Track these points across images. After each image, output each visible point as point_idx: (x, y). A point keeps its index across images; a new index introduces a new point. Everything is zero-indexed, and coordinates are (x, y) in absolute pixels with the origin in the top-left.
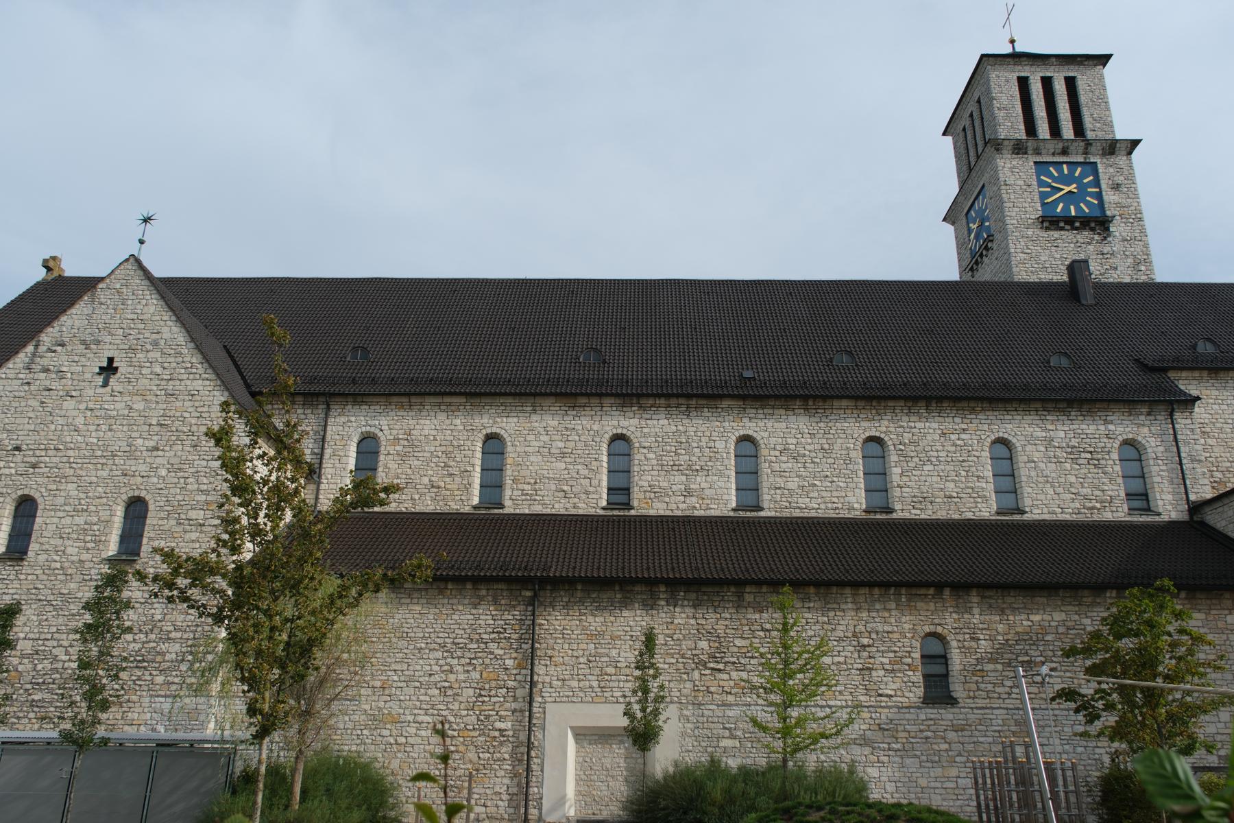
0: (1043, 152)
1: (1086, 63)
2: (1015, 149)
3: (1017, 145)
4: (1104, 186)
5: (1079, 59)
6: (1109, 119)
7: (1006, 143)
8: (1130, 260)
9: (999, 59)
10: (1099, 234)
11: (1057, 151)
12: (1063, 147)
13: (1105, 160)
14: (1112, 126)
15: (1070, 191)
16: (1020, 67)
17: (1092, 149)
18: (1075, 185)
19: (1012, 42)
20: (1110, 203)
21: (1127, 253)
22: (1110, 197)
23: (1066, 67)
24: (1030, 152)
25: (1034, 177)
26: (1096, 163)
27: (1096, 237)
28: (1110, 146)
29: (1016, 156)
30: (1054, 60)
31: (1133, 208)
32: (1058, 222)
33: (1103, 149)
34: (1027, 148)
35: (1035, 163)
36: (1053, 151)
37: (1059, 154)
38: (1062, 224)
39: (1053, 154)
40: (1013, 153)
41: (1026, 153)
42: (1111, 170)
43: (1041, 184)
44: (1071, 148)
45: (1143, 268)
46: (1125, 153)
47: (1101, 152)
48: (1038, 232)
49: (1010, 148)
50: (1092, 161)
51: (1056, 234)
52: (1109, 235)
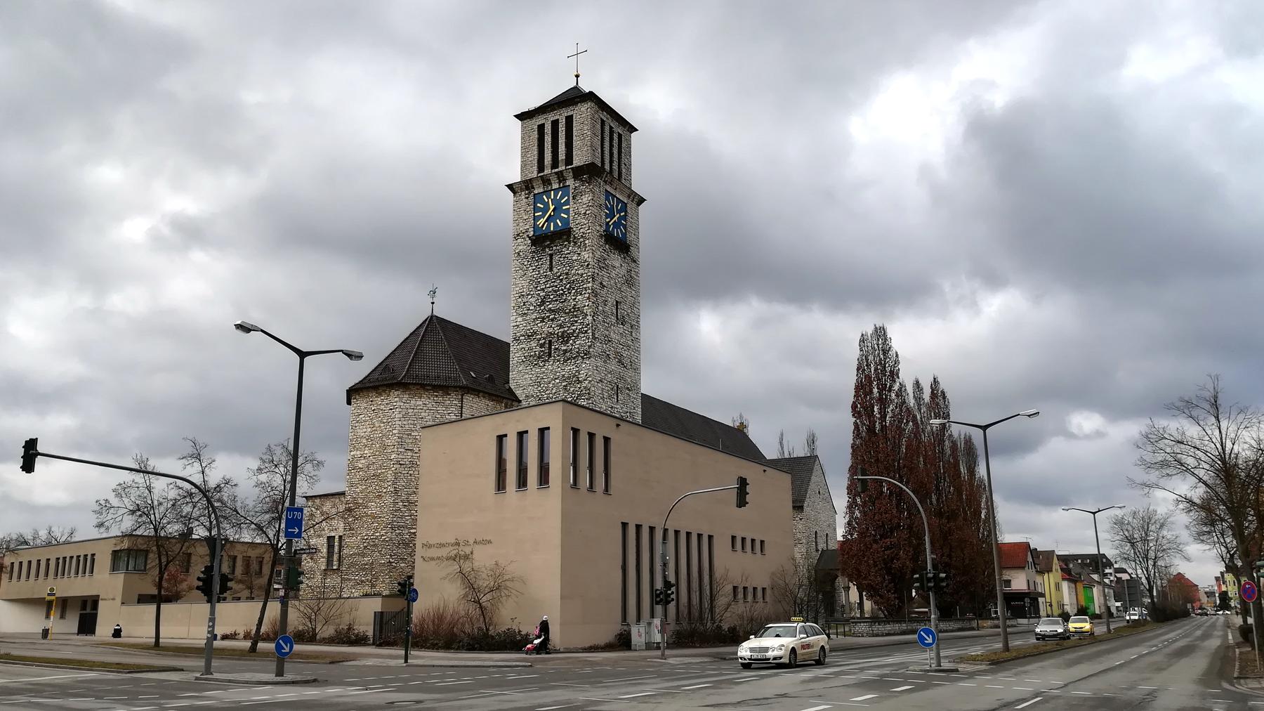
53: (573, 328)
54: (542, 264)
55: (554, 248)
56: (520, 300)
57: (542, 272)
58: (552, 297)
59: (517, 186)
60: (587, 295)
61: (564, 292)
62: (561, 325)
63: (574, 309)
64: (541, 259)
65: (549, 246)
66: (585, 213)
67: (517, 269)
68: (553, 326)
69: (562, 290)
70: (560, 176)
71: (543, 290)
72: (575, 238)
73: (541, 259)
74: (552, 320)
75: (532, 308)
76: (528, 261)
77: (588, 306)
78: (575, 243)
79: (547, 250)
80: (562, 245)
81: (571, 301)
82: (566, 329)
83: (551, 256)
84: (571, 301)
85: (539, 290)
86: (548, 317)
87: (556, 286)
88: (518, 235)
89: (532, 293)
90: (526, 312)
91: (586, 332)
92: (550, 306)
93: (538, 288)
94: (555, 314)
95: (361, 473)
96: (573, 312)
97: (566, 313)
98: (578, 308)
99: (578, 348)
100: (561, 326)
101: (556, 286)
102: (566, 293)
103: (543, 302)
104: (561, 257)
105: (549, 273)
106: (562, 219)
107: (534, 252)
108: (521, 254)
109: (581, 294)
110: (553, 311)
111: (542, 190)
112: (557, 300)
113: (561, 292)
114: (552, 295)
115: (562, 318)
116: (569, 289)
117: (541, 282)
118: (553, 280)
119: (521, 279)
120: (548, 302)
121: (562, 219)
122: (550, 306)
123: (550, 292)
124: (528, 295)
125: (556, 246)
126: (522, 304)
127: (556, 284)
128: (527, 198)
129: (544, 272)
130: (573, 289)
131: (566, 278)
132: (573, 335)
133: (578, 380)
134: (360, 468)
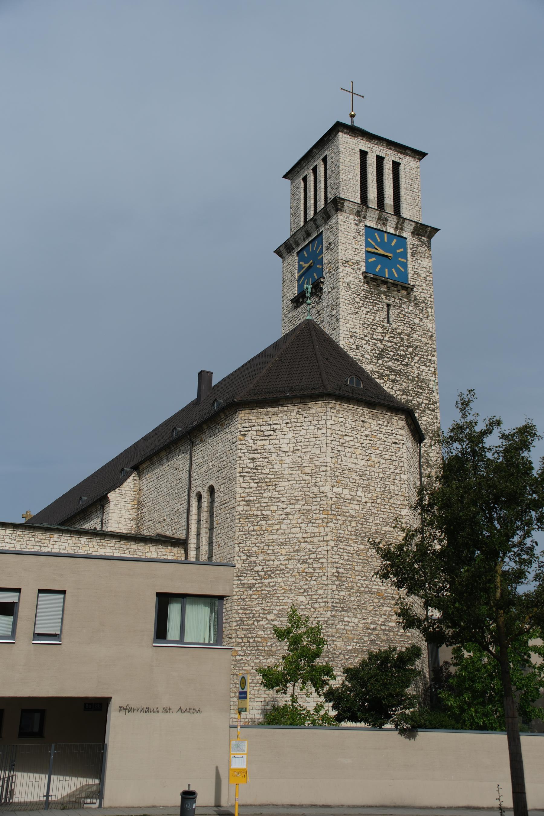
0: (299, 242)
1: (331, 138)
2: (287, 249)
3: (286, 246)
4: (324, 249)
5: (325, 139)
6: (338, 181)
7: (281, 249)
8: (330, 309)
9: (292, 172)
10: (318, 295)
11: (305, 237)
12: (305, 232)
13: (326, 226)
14: (339, 187)
15: (310, 267)
16: (303, 170)
17: (319, 222)
18: (311, 261)
19: (352, 116)
20: (325, 264)
21: (329, 304)
22: (326, 257)
23: (323, 150)
24: (294, 246)
25: (297, 266)
26: (322, 232)
27: (317, 299)
28: (324, 213)
29: (289, 254)
30: (315, 150)
31: (334, 261)
32: (299, 299)
33: (323, 218)
34: (291, 245)
35: (298, 253)
36: (302, 237)
37: (307, 237)
38: (301, 300)
39: (304, 240)
40: (288, 253)
41: (293, 249)
42: (328, 232)
43: (300, 268)
44: (309, 229)
45: (334, 313)
46: (334, 212)
47: (323, 221)
48: (292, 313)
49: (285, 251)
50: (321, 231)
51: (299, 310)
52: (322, 294)
53: (418, 399)
54: (377, 311)
55: (392, 299)
56: (352, 340)
57: (378, 319)
58: (392, 354)
59: (350, 205)
60: (433, 369)
61: (406, 354)
62: (403, 391)
63: (418, 378)
64: (376, 304)
65: (384, 293)
66: (425, 278)
67: (346, 302)
68: (394, 388)
69: (403, 350)
70: (400, 223)
71: (381, 341)
72: (415, 299)
73: (376, 304)
74: (393, 381)
75: (366, 356)
76: (360, 300)
77: (434, 381)
78: (416, 305)
79: (384, 297)
80: (401, 300)
81: (415, 368)
82: (410, 398)
83: (388, 305)
84: (415, 368)
85: (375, 339)
86: (388, 375)
87: (396, 344)
88: (347, 262)
89: (367, 338)
90: (361, 358)
91: (433, 410)
92: (390, 364)
93: (375, 337)
94: (396, 375)
95: (354, 524)
96: (417, 382)
97: (408, 379)
98: (423, 379)
99: (425, 425)
100: (404, 393)
101: (396, 344)
102: (409, 356)
103: (380, 356)
104: (400, 313)
105: (386, 325)
106: (398, 270)
107: (367, 292)
108: (352, 286)
109: (425, 365)
110: (394, 371)
111: (374, 226)
112: (397, 360)
113: (402, 352)
114: (391, 351)
115: (404, 384)
116: (411, 354)
117: (378, 331)
118: (392, 335)
119: (352, 316)
120: (387, 357)
121: (398, 270)
122: (390, 364)
123: (389, 347)
124: (362, 339)
125: (395, 298)
126: (355, 347)
127: (395, 341)
128: (357, 225)
129: (380, 321)
130: (417, 355)
131: (407, 340)
132: (418, 407)
133: (428, 463)
134: (352, 516)
